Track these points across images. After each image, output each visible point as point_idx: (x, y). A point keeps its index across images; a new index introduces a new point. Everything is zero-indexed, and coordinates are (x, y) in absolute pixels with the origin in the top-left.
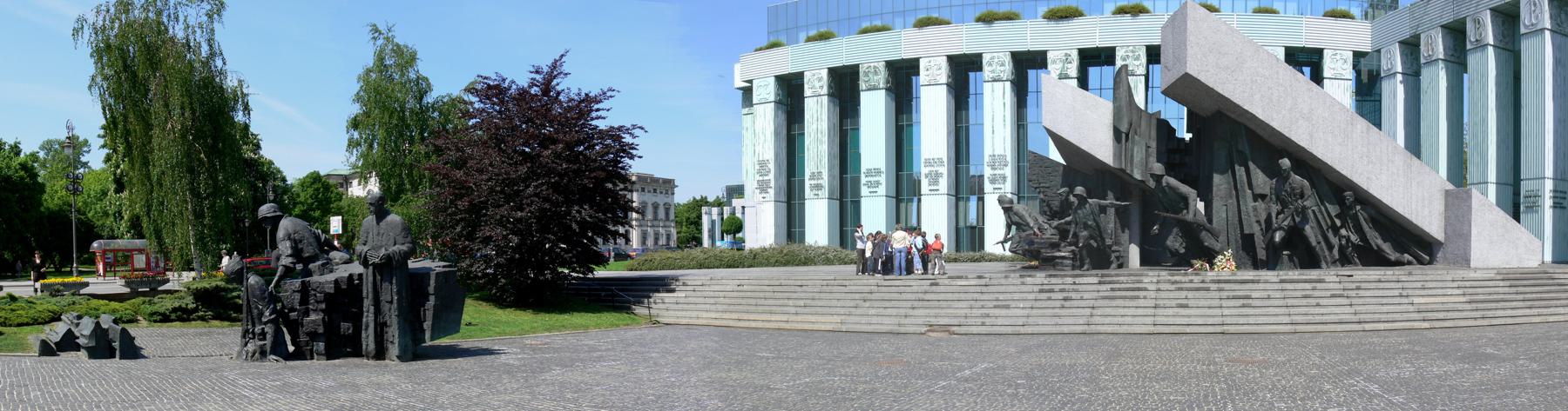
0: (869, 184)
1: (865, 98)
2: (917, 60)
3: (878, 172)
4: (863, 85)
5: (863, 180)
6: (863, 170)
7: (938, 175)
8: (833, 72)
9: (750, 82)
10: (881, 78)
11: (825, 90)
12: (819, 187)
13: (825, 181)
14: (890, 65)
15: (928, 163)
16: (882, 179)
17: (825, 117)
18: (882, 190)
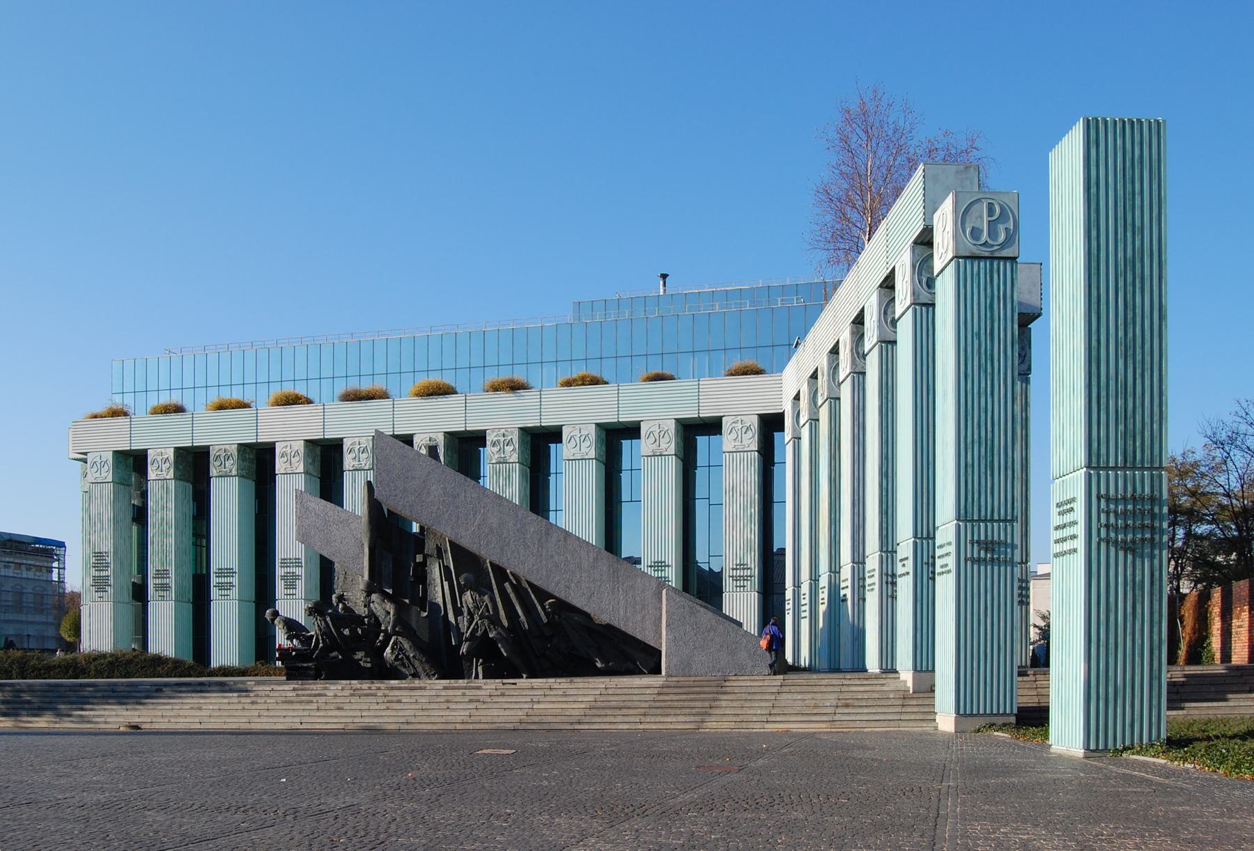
0: (221, 586)
1: (215, 485)
2: (274, 443)
3: (228, 572)
4: (213, 472)
5: (214, 580)
6: (214, 568)
7: (295, 577)
8: (181, 452)
9: (85, 454)
10: (232, 466)
11: (171, 475)
12: (164, 587)
13: (172, 581)
14: (243, 448)
15: (285, 563)
16: (235, 580)
17: (172, 505)
18: (234, 593)
